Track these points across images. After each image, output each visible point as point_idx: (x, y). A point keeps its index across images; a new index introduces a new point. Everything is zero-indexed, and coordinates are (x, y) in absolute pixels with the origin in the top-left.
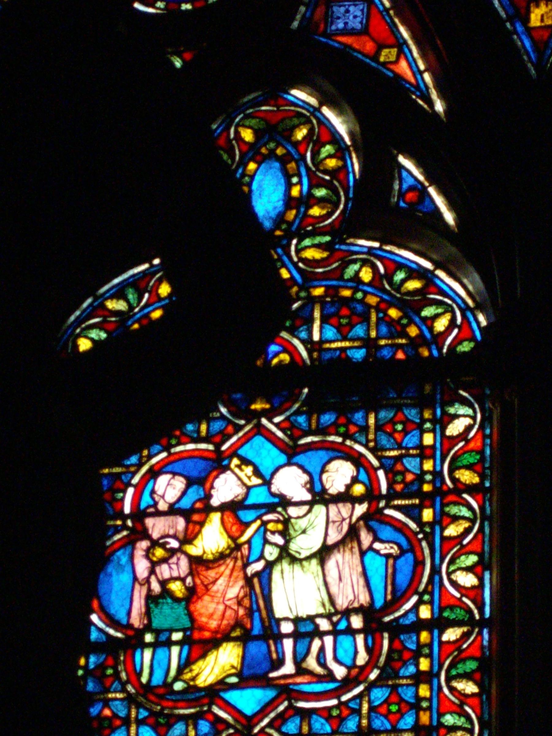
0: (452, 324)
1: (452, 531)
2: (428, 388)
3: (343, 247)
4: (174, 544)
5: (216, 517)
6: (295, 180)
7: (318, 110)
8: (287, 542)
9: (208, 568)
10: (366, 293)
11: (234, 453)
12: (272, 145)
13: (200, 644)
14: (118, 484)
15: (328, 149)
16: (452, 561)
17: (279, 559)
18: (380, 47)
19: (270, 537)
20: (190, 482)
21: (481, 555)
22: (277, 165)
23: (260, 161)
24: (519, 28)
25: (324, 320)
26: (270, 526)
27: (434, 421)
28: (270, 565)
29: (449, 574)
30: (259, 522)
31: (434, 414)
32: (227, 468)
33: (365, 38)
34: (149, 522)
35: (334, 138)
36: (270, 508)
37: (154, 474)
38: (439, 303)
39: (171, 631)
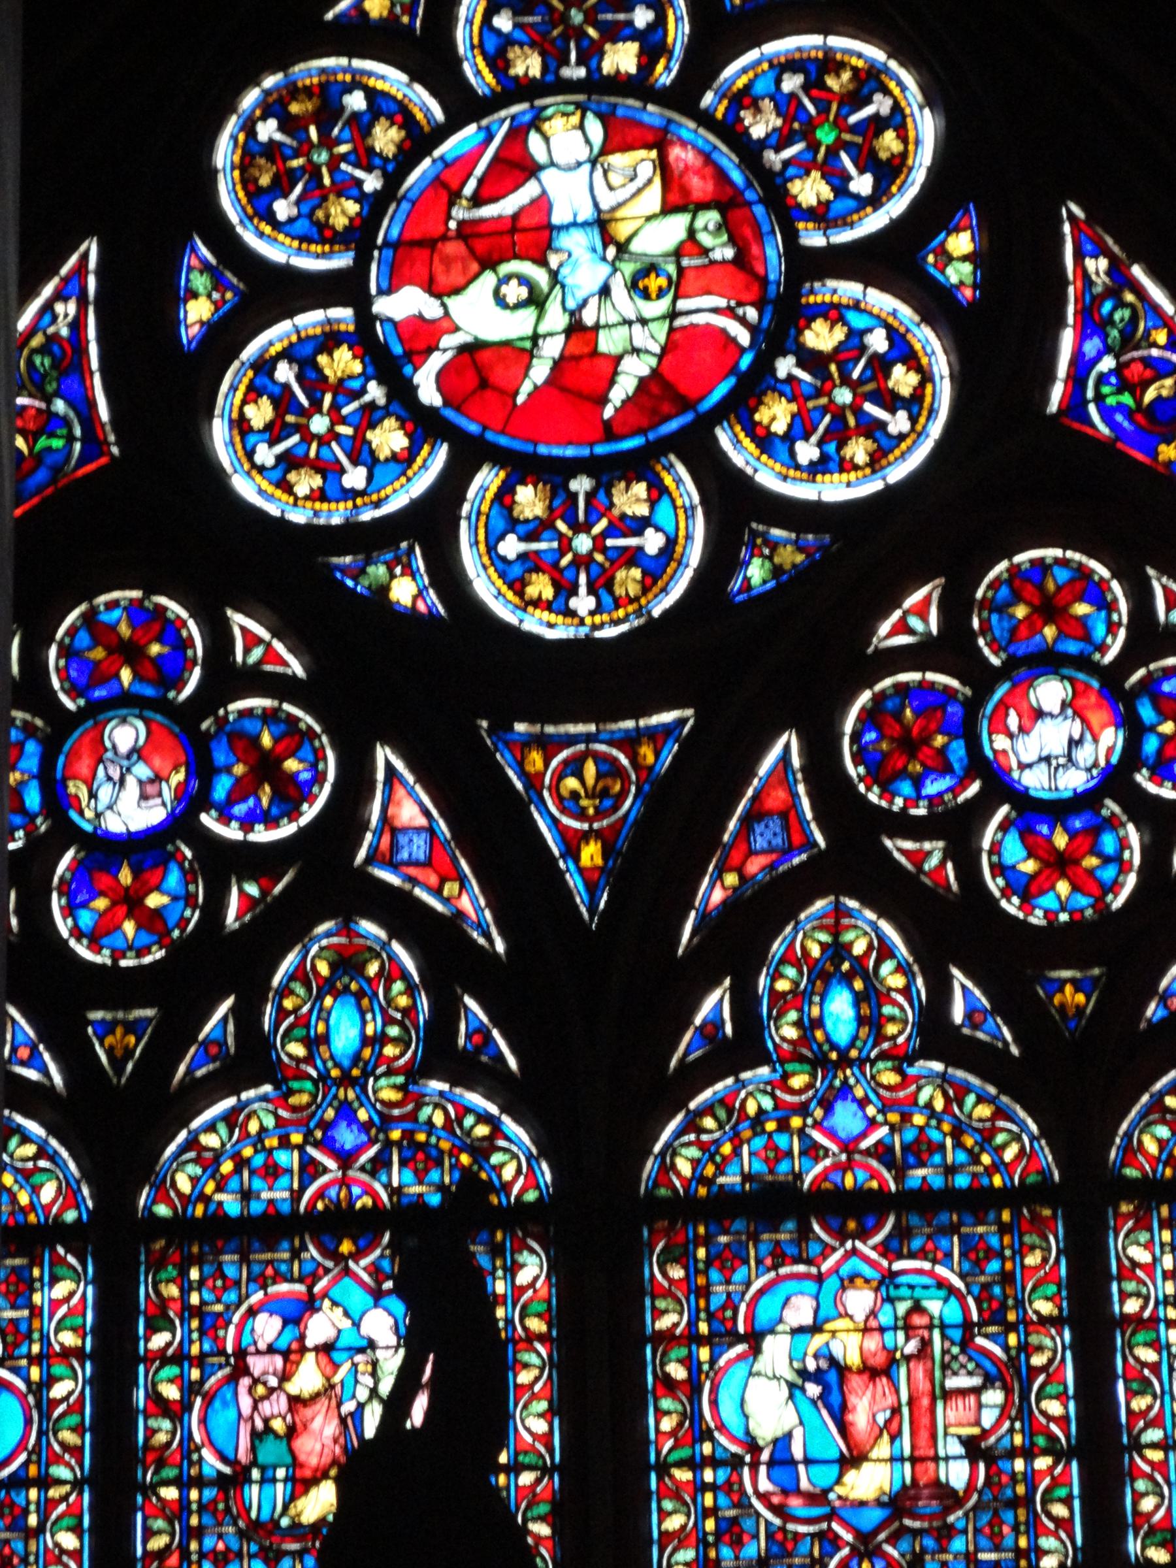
0: (519, 1171)
1: (524, 1377)
2: (499, 1236)
5: (310, 1357)
11: (325, 1294)
12: (346, 979)
13: (301, 1484)
14: (220, 1322)
15: (398, 986)
16: (525, 1407)
17: (370, 1399)
18: (443, 880)
22: (352, 1000)
23: (336, 995)
24: (572, 867)
25: (403, 1163)
26: (361, 1368)
27: (505, 1268)
28: (361, 1406)
34: (251, 1360)
35: (404, 976)
36: (361, 1350)
37: (252, 1312)
38: (505, 1150)
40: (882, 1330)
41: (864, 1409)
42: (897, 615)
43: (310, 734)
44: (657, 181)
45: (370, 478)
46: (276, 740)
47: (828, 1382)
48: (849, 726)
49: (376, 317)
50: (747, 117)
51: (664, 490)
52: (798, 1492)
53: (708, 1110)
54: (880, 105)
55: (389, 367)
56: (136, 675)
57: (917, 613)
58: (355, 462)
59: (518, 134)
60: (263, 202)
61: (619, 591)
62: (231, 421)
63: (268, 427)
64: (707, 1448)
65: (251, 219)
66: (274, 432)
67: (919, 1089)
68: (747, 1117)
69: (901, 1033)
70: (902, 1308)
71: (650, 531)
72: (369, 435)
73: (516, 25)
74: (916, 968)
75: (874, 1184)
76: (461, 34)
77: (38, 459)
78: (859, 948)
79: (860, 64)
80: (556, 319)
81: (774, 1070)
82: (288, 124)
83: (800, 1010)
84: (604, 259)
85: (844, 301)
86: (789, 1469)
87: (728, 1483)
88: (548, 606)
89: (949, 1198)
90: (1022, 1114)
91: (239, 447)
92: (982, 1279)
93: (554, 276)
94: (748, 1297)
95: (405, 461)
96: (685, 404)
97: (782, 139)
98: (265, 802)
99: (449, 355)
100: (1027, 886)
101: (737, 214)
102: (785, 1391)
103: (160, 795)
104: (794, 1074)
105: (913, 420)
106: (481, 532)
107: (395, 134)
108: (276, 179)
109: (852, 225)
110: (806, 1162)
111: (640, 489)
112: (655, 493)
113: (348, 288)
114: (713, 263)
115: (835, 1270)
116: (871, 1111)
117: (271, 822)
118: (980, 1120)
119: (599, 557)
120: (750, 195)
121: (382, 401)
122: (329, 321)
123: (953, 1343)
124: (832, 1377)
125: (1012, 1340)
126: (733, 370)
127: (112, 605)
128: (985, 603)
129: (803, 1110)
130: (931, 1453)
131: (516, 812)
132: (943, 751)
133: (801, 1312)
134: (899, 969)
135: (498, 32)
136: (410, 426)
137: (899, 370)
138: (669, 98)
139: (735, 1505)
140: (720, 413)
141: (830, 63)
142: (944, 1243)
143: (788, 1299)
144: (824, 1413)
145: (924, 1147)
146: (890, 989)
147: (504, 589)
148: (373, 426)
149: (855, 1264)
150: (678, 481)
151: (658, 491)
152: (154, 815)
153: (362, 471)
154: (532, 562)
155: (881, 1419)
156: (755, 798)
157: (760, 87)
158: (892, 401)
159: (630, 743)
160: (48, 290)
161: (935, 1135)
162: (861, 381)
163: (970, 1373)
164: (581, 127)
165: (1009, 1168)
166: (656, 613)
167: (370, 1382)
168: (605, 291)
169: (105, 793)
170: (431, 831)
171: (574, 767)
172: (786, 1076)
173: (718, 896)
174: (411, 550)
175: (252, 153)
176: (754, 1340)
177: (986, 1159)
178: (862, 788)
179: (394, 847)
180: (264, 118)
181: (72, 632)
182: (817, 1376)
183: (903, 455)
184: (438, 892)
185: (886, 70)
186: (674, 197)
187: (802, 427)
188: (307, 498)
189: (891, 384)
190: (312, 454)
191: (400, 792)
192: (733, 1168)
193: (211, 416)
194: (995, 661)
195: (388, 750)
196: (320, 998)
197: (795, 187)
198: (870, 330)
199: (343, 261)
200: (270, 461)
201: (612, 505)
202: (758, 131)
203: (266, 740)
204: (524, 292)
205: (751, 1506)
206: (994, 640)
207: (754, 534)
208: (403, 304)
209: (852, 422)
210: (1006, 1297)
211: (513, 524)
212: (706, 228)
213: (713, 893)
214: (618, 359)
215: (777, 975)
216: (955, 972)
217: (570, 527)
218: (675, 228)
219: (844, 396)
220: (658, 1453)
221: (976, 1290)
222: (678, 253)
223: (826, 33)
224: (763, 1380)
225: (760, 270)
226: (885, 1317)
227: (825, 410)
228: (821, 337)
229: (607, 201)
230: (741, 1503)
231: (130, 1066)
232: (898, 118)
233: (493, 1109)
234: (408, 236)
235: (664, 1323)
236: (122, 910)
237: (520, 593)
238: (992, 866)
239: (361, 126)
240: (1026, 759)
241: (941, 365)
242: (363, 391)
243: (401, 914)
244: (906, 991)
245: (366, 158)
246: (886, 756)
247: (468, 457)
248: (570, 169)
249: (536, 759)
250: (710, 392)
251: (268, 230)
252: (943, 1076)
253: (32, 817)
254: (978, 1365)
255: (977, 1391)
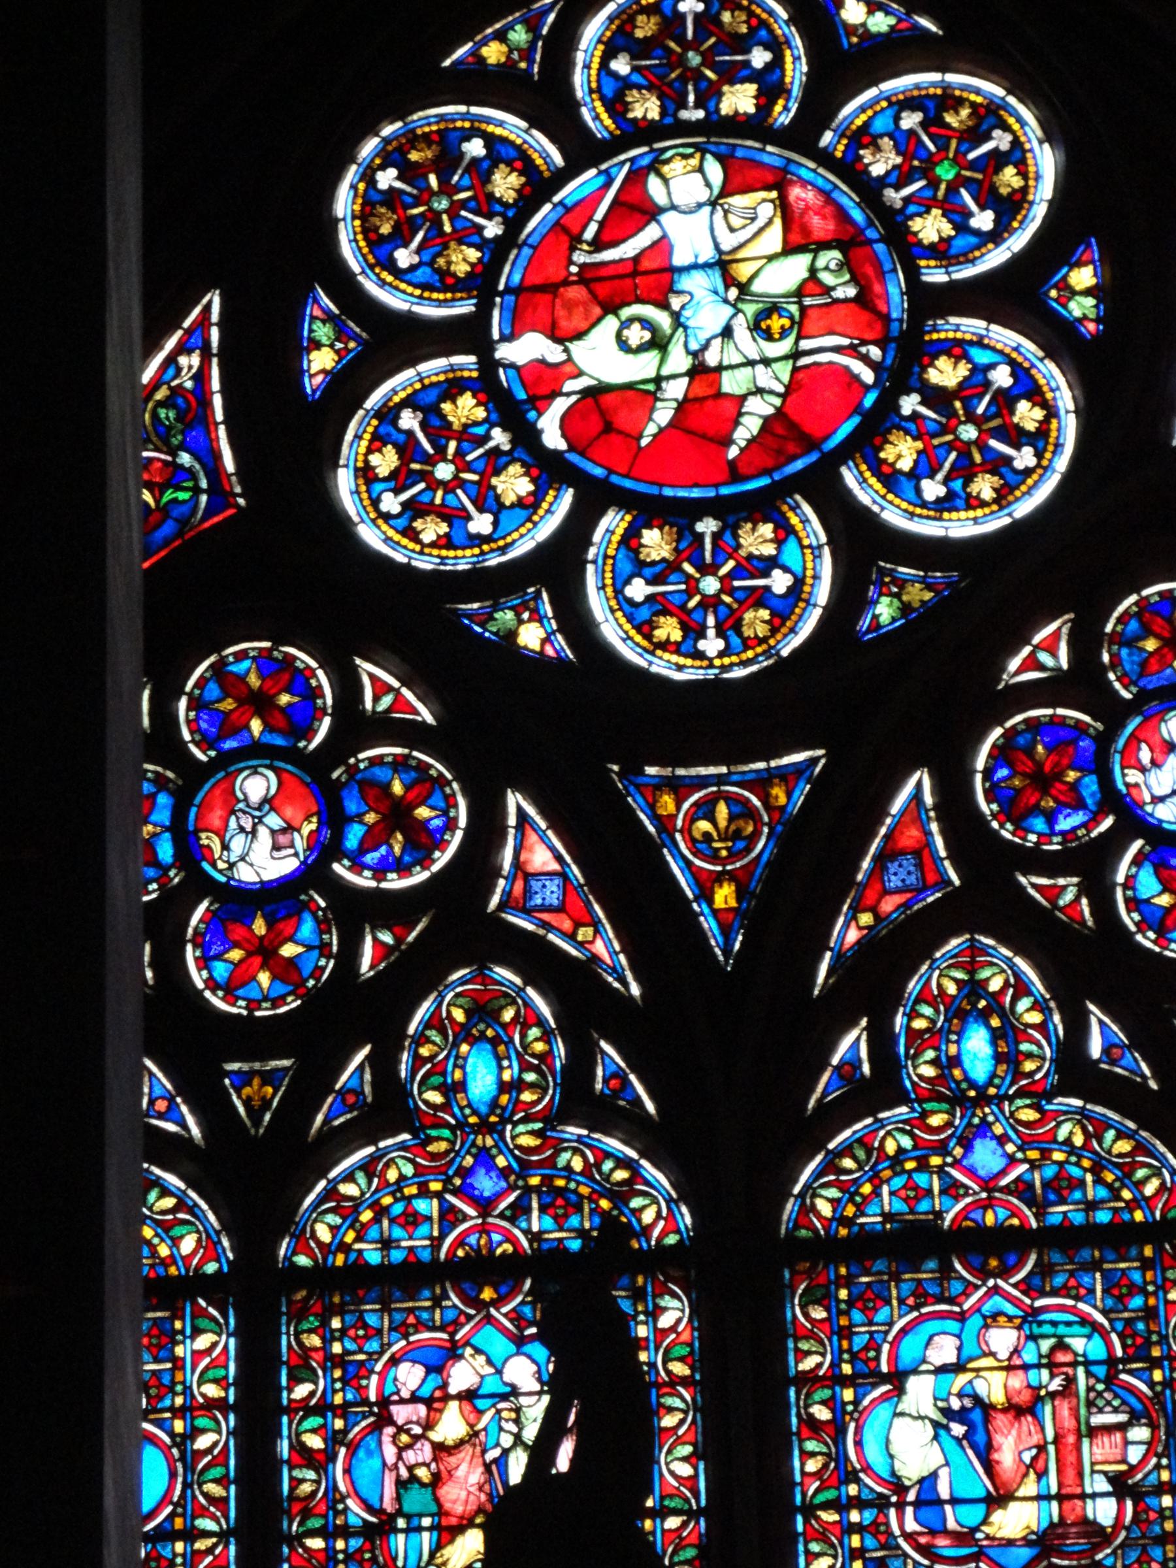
0: (659, 1215)
1: (668, 1421)
2: (640, 1280)
3: (554, 1134)
4: (417, 1430)
5: (453, 1405)
6: (505, 1063)
7: (523, 990)
8: (521, 1429)
9: (450, 1454)
10: (578, 1183)
12: (482, 1026)
14: (363, 1372)
15: (534, 1032)
16: (669, 1452)
18: (577, 924)
19: (503, 1424)
20: (429, 1370)
21: (695, 1445)
22: (488, 1047)
23: (473, 1041)
25: (543, 1209)
26: (505, 1414)
27: (646, 1313)
28: (506, 1452)
29: (667, 1464)
30: (493, 1410)
31: (646, 1306)
32: (461, 1357)
33: (564, 916)
34: (394, 1409)
35: (540, 1022)
36: (504, 1397)
37: (394, 1361)
39: (421, 1516)
40: (1026, 1367)
41: (1010, 1448)
42: (1027, 650)
43: (441, 781)
44: (778, 222)
45: (496, 524)
46: (408, 788)
47: (971, 1422)
48: (980, 763)
49: (499, 363)
50: (866, 155)
51: (790, 531)
52: (946, 1532)
53: (846, 1150)
54: (1000, 141)
55: (514, 414)
56: (268, 727)
57: (1048, 647)
58: (481, 510)
59: (637, 177)
60: (383, 251)
61: (748, 632)
62: (356, 469)
63: (394, 475)
64: (853, 1490)
65: (371, 267)
66: (399, 480)
67: (1059, 1124)
68: (888, 1157)
69: (1039, 1069)
70: (1046, 1345)
71: (777, 573)
72: (494, 481)
73: (635, 69)
74: (1052, 1004)
75: (1016, 1222)
76: (579, 79)
77: (164, 511)
78: (995, 985)
79: (979, 99)
80: (678, 361)
81: (913, 1110)
82: (409, 172)
83: (937, 1048)
84: (726, 301)
85: (968, 337)
86: (937, 1508)
87: (875, 1523)
88: (676, 648)
89: (1091, 1234)
90: (1162, 1149)
91: (365, 496)
92: (1126, 1315)
93: (676, 316)
94: (890, 1338)
95: (530, 505)
96: (811, 444)
97: (902, 176)
98: (397, 849)
99: (574, 398)
100: (1162, 921)
101: (858, 253)
102: (931, 1432)
103: (292, 846)
104: (933, 1112)
105: (1039, 455)
106: (609, 575)
107: (515, 180)
108: (396, 227)
109: (973, 261)
110: (947, 1201)
111: (767, 529)
112: (782, 534)
113: (470, 335)
114: (836, 301)
115: (977, 1309)
116: (1010, 1148)
117: (404, 870)
118: (1120, 1155)
119: (727, 599)
120: (871, 234)
121: (506, 447)
122: (452, 369)
123: (1098, 1381)
124: (977, 1416)
125: (1157, 1375)
126: (858, 409)
127: (241, 656)
128: (1116, 638)
129: (942, 1148)
130: (1078, 1490)
131: (647, 855)
132: (1075, 786)
133: (944, 1351)
134: (1036, 1006)
135: (615, 75)
136: (535, 472)
137: (1023, 406)
138: (787, 138)
139: (883, 1547)
140: (845, 452)
141: (949, 100)
142: (1086, 1280)
143: (931, 1338)
144: (970, 1452)
145: (1064, 1184)
146: (1028, 1026)
147: (632, 633)
148: (497, 472)
149: (997, 1302)
150: (805, 521)
151: (784, 532)
152: (287, 865)
153: (488, 518)
154: (659, 605)
155: (1027, 1457)
156: (886, 837)
157: (879, 125)
158: (1017, 437)
159: (760, 784)
160: (171, 343)
161: (1075, 1171)
162: (986, 418)
163: (1116, 1410)
164: (700, 169)
165: (1150, 1202)
166: (785, 653)
167: (515, 1430)
168: (727, 332)
169: (238, 844)
170: (563, 876)
171: (705, 809)
172: (925, 1114)
173: (853, 936)
174: (537, 596)
175: (372, 202)
176: (897, 1379)
177: (1126, 1194)
178: (995, 825)
179: (528, 893)
180: (383, 167)
181: (201, 683)
182: (961, 1416)
183: (1028, 492)
184: (571, 937)
185: (1005, 106)
186: (796, 238)
187: (927, 465)
188: (433, 545)
189: (1016, 420)
190: (438, 501)
191: (532, 838)
192: (873, 1209)
193: (336, 465)
194: (1127, 695)
195: (518, 796)
196: (456, 1045)
197: (916, 224)
198: (992, 366)
199: (465, 308)
200: (396, 509)
201: (739, 546)
202: (877, 170)
203: (397, 788)
204: (647, 335)
205: (898, 1547)
206: (1125, 674)
207: (882, 572)
208: (527, 349)
209: (978, 458)
210: (1150, 1332)
211: (640, 567)
212: (827, 268)
213: (848, 932)
214: (743, 398)
215: (913, 1015)
216: (1092, 1007)
217: (698, 569)
218: (796, 268)
219: (969, 432)
220: (804, 1494)
221: (1119, 1326)
222: (799, 293)
223: (943, 70)
224: (907, 1419)
225: (883, 308)
226: (1029, 1355)
227: (950, 446)
228: (946, 374)
229: (728, 242)
230: (889, 1544)
231: (267, 1117)
232: (1018, 154)
233: (633, 1154)
234: (528, 282)
235: (808, 1364)
236: (257, 960)
237: (648, 637)
238: (1127, 901)
239: (481, 172)
240: (1159, 792)
241: (1065, 400)
242: (487, 437)
243: (537, 960)
244: (1042, 1027)
245: (487, 205)
246: (1018, 791)
247: (593, 500)
248: (691, 212)
249: (667, 803)
250: (834, 432)
251: (390, 279)
252: (1082, 1111)
253: (165, 869)
254: (1124, 1402)
255: (1122, 1427)
